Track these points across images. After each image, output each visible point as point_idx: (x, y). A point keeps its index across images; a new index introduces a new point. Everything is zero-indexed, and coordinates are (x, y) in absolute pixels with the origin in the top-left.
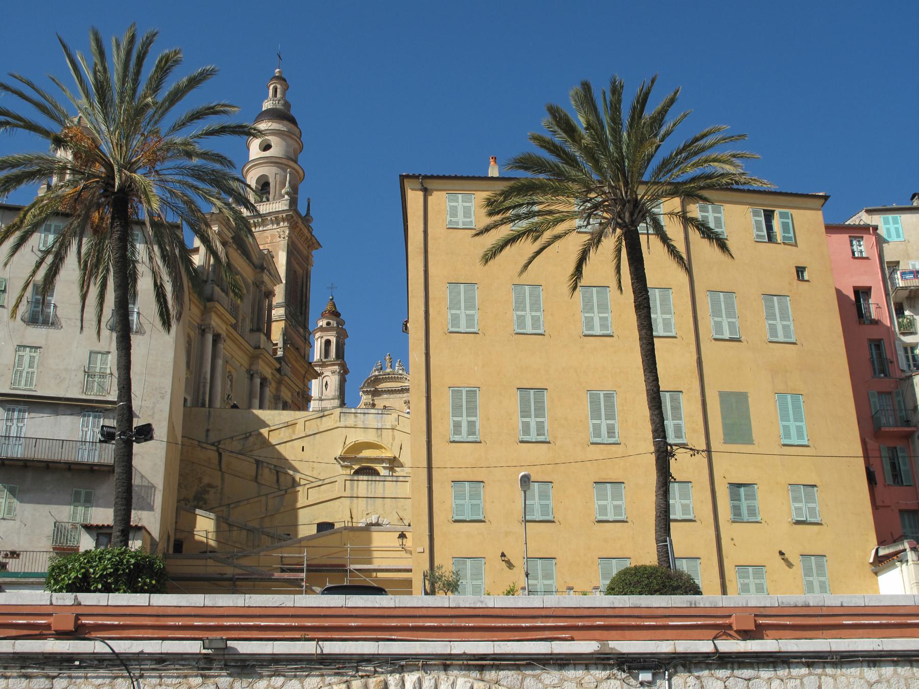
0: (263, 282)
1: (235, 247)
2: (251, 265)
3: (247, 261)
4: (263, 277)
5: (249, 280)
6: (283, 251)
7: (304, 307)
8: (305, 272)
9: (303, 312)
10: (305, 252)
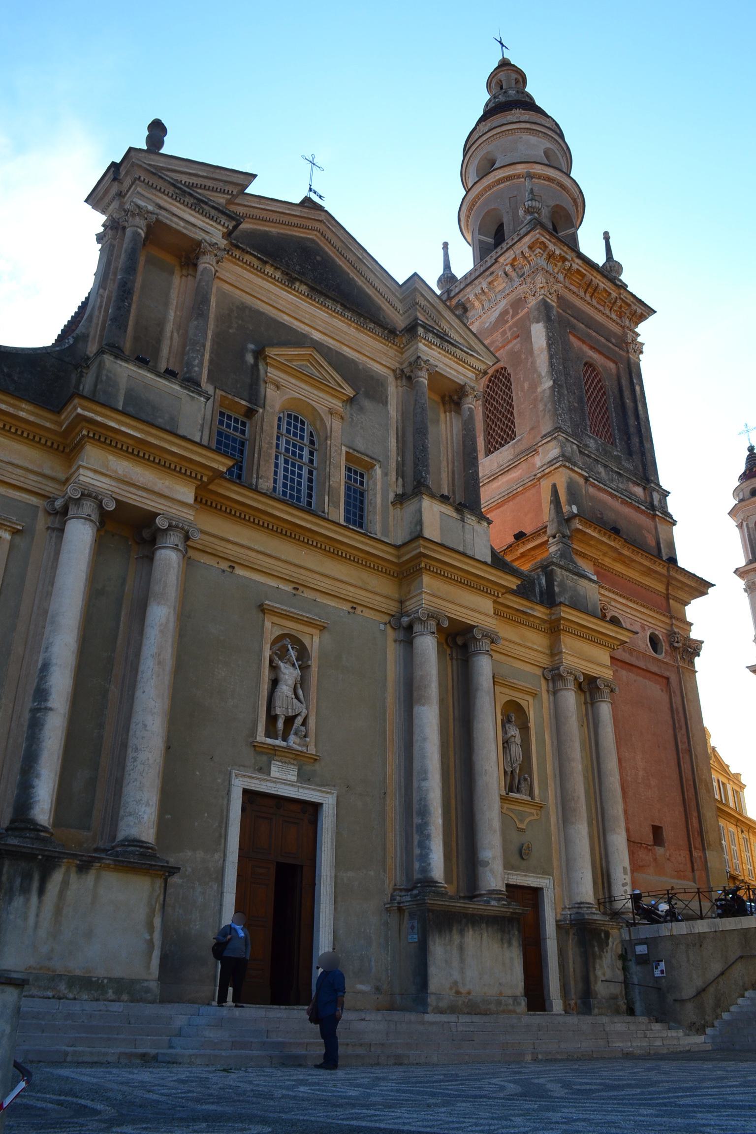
1: (278, 275)
4: (417, 349)
6: (538, 322)
7: (635, 440)
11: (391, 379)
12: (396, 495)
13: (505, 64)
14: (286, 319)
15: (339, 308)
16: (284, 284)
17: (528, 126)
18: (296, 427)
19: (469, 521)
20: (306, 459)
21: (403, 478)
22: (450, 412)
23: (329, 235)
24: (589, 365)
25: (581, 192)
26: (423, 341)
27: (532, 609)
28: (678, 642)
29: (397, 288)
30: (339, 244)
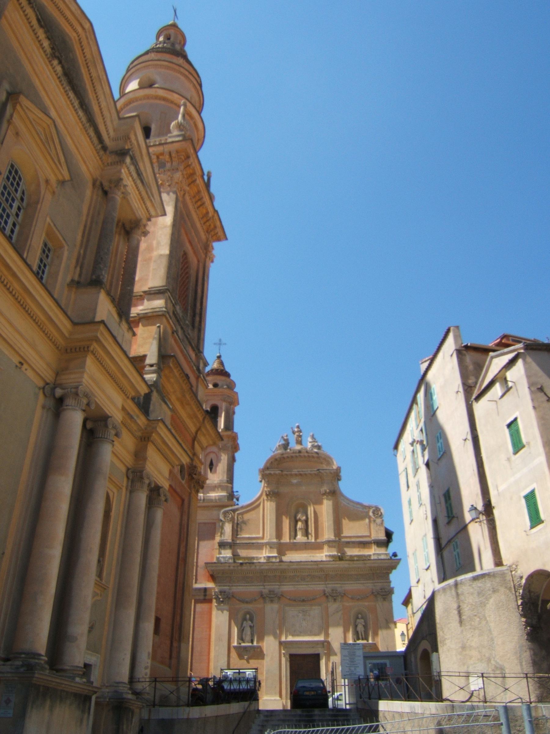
0: (118, 182)
2: (92, 134)
3: (81, 113)
4: (120, 172)
5: (84, 168)
7: (197, 319)
8: (201, 265)
9: (197, 324)
10: (203, 236)
11: (90, 185)
12: (72, 281)
13: (174, 26)
14: (37, 83)
15: (76, 104)
16: (46, 55)
17: (187, 73)
18: (14, 179)
19: (123, 327)
20: (14, 210)
21: (81, 268)
22: (120, 234)
23: (85, 43)
24: (185, 254)
25: (204, 137)
26: (126, 170)
27: (138, 416)
28: (195, 474)
29: (117, 118)
30: (88, 56)
